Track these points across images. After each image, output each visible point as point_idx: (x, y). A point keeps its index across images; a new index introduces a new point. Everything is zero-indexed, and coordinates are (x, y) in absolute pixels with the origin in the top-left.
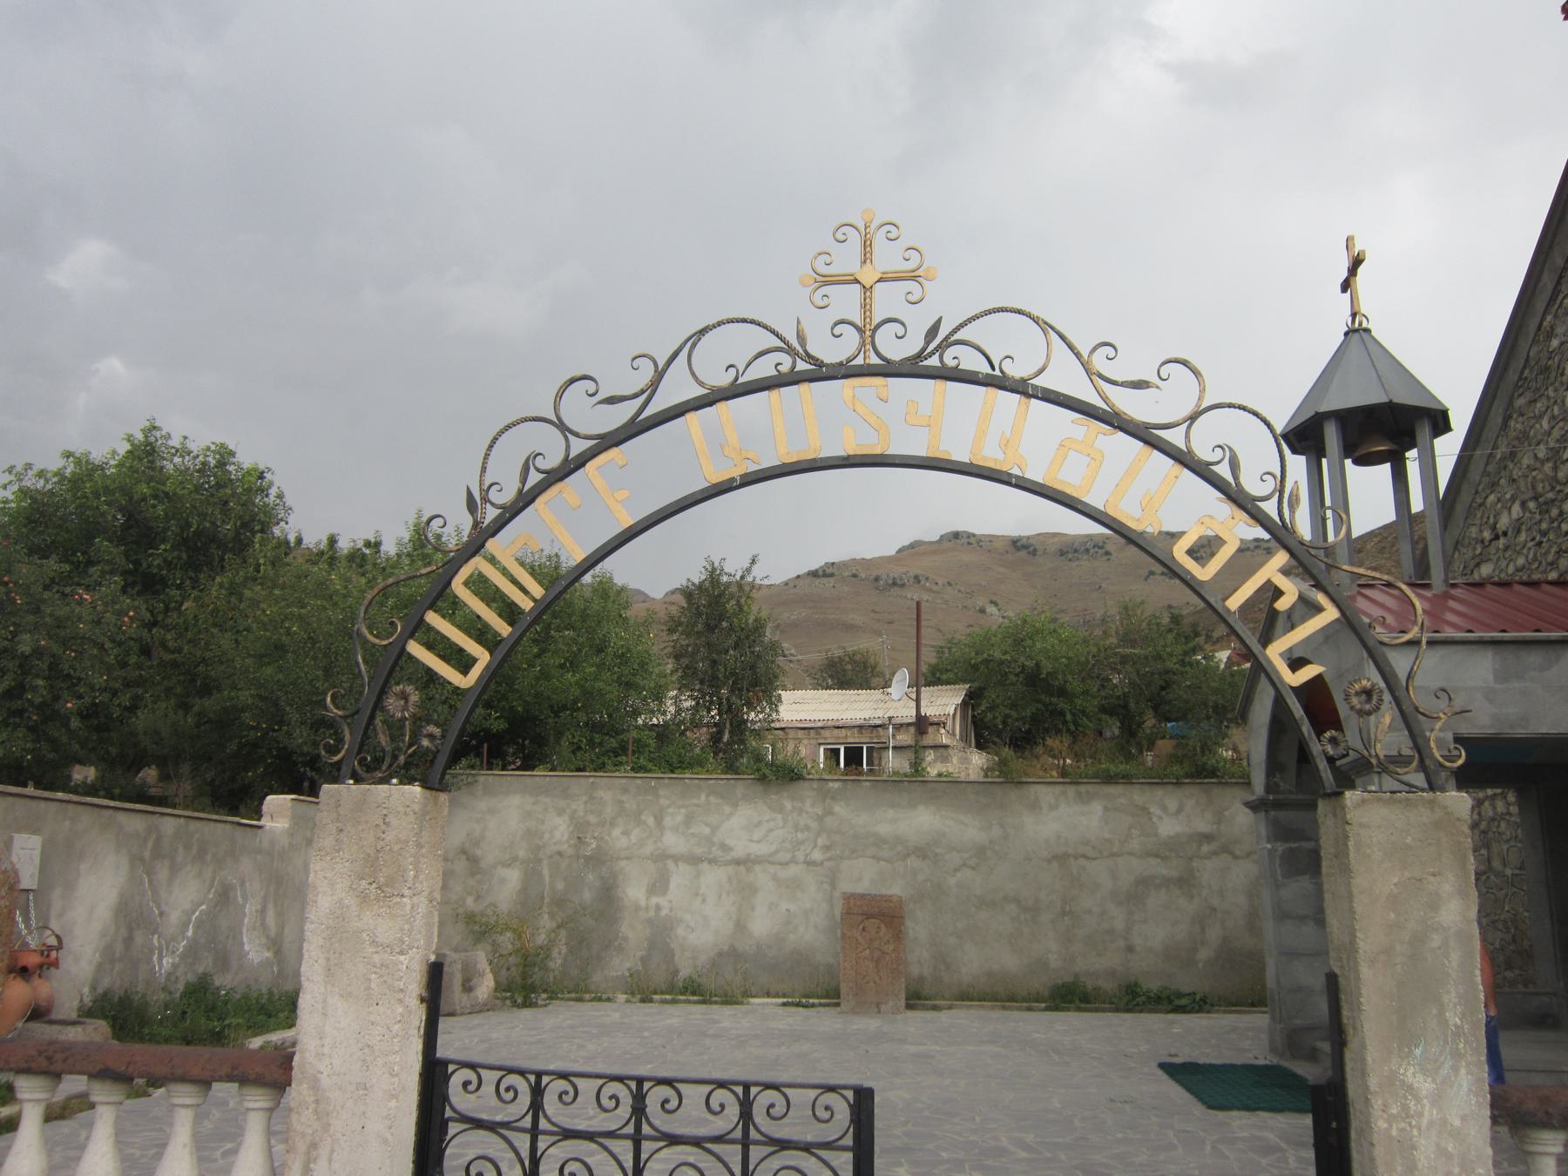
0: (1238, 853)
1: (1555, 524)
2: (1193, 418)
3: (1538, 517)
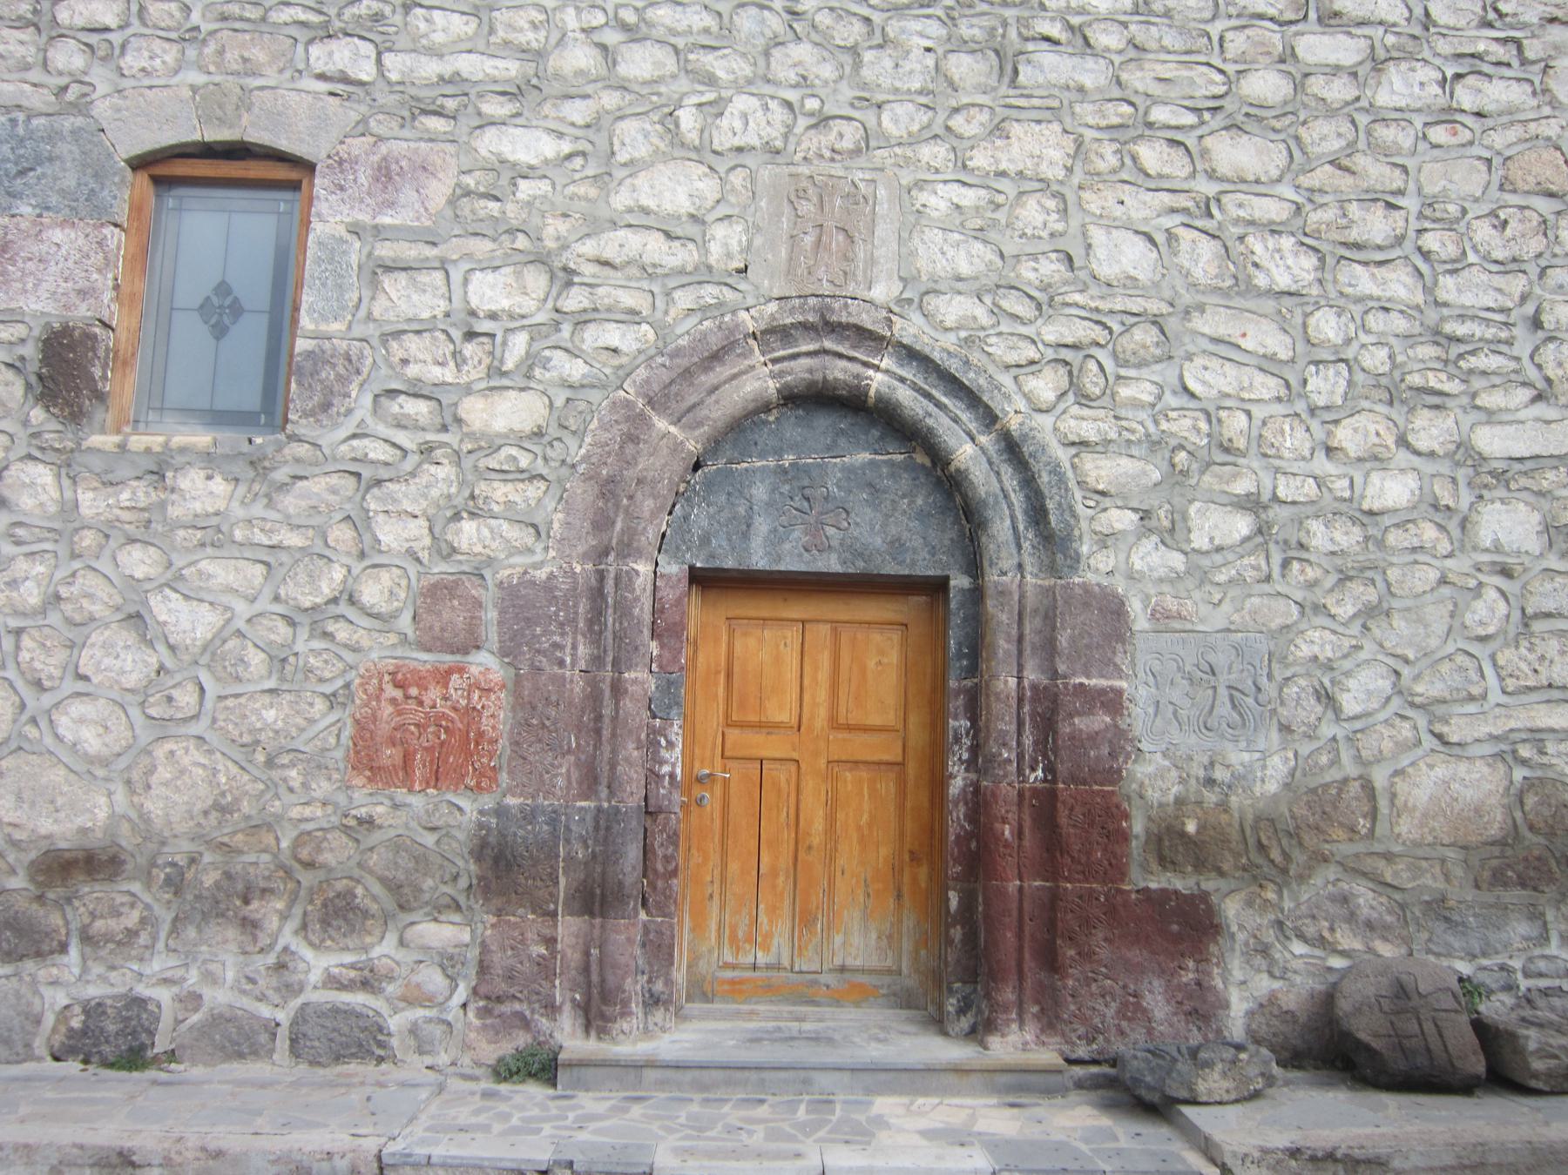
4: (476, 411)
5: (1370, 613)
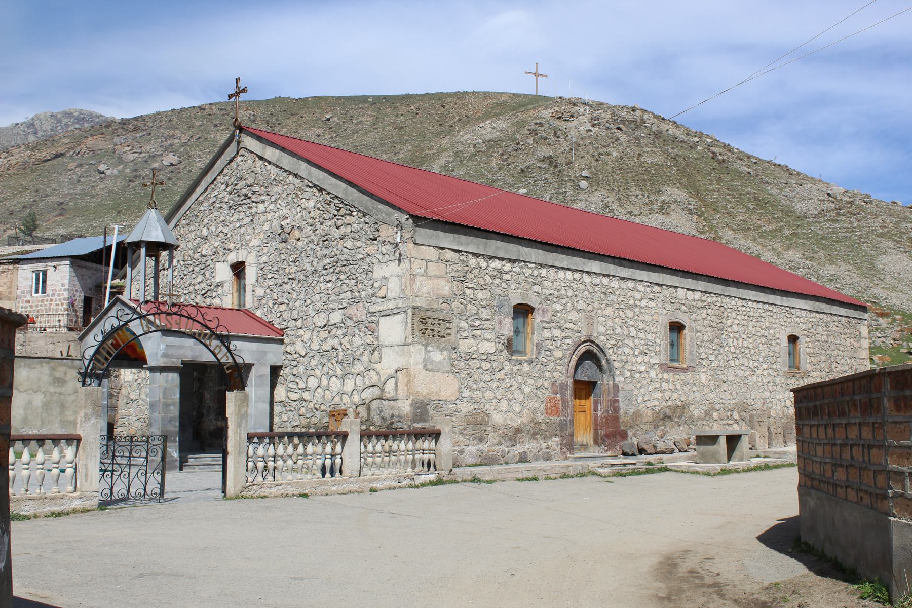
0: (21, 389)
1: (190, 273)
2: (217, 328)
3: (184, 268)
4: (555, 353)
5: (641, 387)
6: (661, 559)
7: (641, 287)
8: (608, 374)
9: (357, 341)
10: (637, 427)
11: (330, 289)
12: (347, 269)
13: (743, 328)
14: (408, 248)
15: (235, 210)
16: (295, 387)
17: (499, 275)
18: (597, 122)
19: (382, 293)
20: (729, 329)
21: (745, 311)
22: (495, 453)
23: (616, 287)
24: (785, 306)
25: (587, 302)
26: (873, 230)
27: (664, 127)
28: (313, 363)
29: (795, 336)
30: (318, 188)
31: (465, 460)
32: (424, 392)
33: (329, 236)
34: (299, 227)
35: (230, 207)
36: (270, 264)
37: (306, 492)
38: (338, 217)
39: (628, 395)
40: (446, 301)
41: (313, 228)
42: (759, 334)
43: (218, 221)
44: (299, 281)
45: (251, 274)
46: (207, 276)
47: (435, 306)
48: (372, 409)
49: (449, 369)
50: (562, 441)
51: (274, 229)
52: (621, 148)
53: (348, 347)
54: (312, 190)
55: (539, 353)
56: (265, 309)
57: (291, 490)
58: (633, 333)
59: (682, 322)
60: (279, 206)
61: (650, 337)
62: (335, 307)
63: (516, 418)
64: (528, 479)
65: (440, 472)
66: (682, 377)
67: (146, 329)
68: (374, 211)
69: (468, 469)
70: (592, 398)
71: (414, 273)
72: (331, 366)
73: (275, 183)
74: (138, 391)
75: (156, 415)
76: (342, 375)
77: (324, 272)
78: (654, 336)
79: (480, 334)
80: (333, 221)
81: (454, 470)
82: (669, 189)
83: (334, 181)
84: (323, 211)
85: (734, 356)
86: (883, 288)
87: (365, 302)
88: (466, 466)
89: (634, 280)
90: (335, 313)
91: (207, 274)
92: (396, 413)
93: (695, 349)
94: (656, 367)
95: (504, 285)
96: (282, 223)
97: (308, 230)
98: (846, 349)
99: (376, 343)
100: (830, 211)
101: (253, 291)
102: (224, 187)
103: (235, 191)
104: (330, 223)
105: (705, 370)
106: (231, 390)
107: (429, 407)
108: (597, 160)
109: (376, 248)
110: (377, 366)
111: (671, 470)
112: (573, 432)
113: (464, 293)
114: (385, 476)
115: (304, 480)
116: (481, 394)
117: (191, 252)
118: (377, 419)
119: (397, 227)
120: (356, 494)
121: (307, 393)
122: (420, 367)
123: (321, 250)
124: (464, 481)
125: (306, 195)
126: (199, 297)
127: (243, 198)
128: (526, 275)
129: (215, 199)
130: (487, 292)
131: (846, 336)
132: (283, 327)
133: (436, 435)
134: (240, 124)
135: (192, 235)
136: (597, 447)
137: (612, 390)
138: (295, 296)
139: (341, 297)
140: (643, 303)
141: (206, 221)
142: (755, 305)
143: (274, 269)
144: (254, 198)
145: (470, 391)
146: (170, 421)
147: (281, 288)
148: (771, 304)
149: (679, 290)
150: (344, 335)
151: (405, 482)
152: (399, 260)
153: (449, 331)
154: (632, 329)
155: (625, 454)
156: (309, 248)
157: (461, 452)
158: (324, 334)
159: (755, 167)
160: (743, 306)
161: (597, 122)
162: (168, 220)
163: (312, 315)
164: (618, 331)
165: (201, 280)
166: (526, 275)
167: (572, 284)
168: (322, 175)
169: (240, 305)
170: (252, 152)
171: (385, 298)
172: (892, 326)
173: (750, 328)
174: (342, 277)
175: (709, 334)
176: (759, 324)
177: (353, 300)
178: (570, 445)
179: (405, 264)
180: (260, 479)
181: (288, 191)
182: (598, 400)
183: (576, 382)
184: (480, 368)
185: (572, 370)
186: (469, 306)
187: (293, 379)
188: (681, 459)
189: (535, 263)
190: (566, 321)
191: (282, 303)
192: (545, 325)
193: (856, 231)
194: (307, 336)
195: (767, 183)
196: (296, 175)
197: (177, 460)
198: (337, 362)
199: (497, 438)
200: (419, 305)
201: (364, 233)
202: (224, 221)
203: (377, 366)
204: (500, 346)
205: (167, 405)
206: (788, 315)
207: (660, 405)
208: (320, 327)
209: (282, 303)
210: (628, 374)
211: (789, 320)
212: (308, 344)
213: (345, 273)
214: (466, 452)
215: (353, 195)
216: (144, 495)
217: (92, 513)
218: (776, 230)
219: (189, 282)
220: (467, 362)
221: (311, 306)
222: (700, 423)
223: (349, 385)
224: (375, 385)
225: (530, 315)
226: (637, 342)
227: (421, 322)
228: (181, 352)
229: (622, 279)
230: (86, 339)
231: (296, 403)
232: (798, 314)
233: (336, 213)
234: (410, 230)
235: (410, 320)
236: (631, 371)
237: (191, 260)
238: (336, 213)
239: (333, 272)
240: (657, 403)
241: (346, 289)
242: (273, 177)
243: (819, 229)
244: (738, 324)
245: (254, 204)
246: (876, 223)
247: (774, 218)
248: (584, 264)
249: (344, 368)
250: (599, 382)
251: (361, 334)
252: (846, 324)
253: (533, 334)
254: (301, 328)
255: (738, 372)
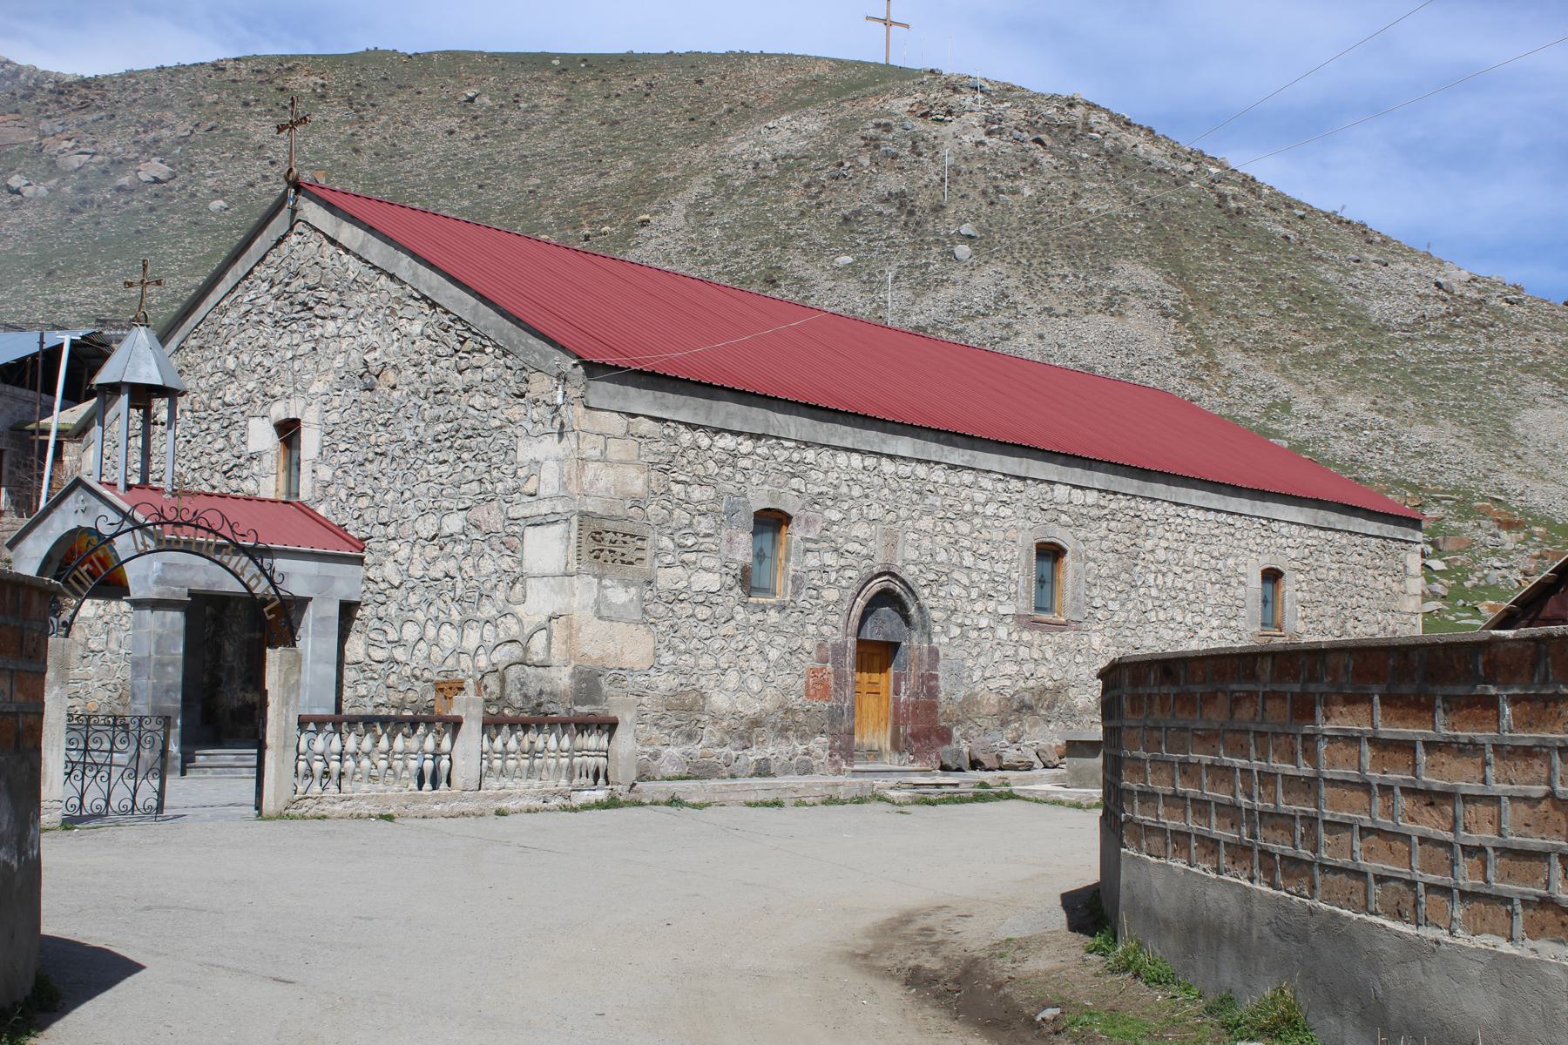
1: (203, 434)
3: (192, 425)
4: (825, 593)
5: (979, 654)
6: (897, 915)
7: (986, 482)
8: (919, 630)
9: (487, 565)
10: (969, 722)
11: (445, 475)
12: (473, 443)
13: (1175, 556)
14: (575, 415)
15: (285, 327)
16: (381, 638)
17: (730, 461)
18: (996, 126)
19: (530, 488)
20: (1148, 556)
21: (1181, 525)
22: (714, 759)
23: (941, 481)
24: (1259, 517)
25: (887, 507)
26: (1515, 358)
27: (1129, 139)
28: (413, 599)
29: (1277, 570)
30: (429, 302)
31: (662, 770)
32: (595, 654)
33: (445, 385)
34: (394, 367)
35: (276, 322)
36: (344, 426)
37: (391, 811)
38: (461, 354)
39: (955, 667)
40: (637, 503)
41: (418, 369)
42: (1206, 566)
43: (255, 344)
44: (393, 459)
45: (310, 441)
46: (234, 440)
47: (619, 512)
48: (508, 681)
49: (640, 618)
50: (832, 742)
51: (353, 366)
52: (1040, 180)
53: (472, 574)
54: (418, 304)
55: (796, 593)
56: (334, 504)
57: (366, 808)
58: (968, 560)
59: (1060, 542)
60: (361, 328)
61: (999, 568)
62: (451, 506)
63: (752, 701)
64: (766, 804)
65: (615, 787)
66: (1057, 639)
67: (141, 547)
68: (522, 347)
69: (666, 783)
70: (891, 671)
71: (584, 456)
72: (442, 606)
73: (355, 287)
74: (104, 637)
75: (143, 681)
76: (461, 621)
77: (435, 445)
78: (1006, 566)
79: (693, 559)
80: (453, 360)
81: (639, 785)
82: (1127, 265)
83: (455, 291)
84: (436, 341)
85: (1157, 603)
86: (1520, 472)
87: (502, 501)
88: (664, 779)
89: (973, 469)
90: (452, 516)
91: (233, 438)
92: (547, 688)
93: (1082, 590)
94: (1009, 620)
95: (739, 477)
96: (365, 357)
97: (410, 372)
98: (1377, 595)
99: (518, 570)
100: (1437, 319)
101: (314, 471)
102: (266, 285)
103: (286, 295)
104: (447, 364)
105: (1101, 626)
106: (274, 646)
107: (602, 679)
108: (992, 203)
109: (523, 411)
110: (519, 609)
111: (1018, 797)
112: (853, 729)
113: (669, 489)
114: (520, 791)
115: (389, 793)
116: (693, 660)
117: (205, 397)
118: (515, 696)
119: (558, 377)
120: (473, 818)
121: (401, 649)
122: (590, 613)
123: (431, 408)
124: (655, 803)
125: (407, 312)
126: (217, 476)
127: (299, 308)
128: (779, 460)
129: (250, 307)
130: (709, 489)
131: (1376, 573)
132: (363, 535)
133: (610, 726)
134: (297, 178)
135: (208, 367)
136: (897, 756)
137: (925, 658)
138: (384, 484)
139: (462, 491)
140: (990, 510)
141: (233, 344)
142: (1201, 515)
143: (351, 435)
144: (318, 310)
145: (674, 654)
146: (167, 691)
147: (362, 468)
148: (1233, 513)
149: (1057, 487)
150: (466, 555)
151: (555, 802)
152: (561, 434)
153: (640, 554)
154: (967, 554)
155: (945, 768)
156: (411, 404)
157: (655, 756)
158: (432, 551)
159: (1301, 225)
160: (1178, 516)
161: (996, 126)
162: (163, 339)
163: (413, 517)
164: (942, 556)
165: (221, 447)
166: (780, 460)
167: (860, 477)
168: (436, 279)
169: (289, 494)
170: (317, 230)
171: (535, 495)
172: (1524, 547)
173: (1190, 554)
174: (465, 456)
175: (1111, 565)
176: (1206, 549)
177: (481, 497)
178: (845, 749)
179: (570, 441)
180: (316, 788)
181: (378, 303)
182: (901, 675)
183: (861, 643)
184: (693, 616)
185: (855, 622)
186: (677, 512)
187: (378, 624)
188: (1041, 780)
189: (796, 441)
190: (846, 539)
191: (363, 495)
192: (809, 545)
193: (1483, 360)
194: (404, 552)
195: (1320, 258)
196: (392, 277)
197: (176, 758)
198: (453, 600)
199: (718, 735)
200: (591, 509)
201: (503, 383)
202: (264, 346)
203: (519, 609)
204: (729, 581)
205: (162, 665)
206: (1264, 533)
207: (1014, 685)
208: (426, 539)
209: (363, 495)
210: (956, 631)
211: (1266, 542)
212: (405, 567)
213: (470, 449)
214: (663, 756)
215: (488, 319)
216: (133, 809)
217: (52, 833)
218: (1327, 353)
219: (200, 449)
220: (670, 606)
221: (411, 502)
222: (1087, 718)
223: (472, 639)
224: (515, 641)
225: (784, 527)
226: (975, 576)
227: (594, 538)
228: (188, 575)
229: (953, 467)
230: (19, 546)
231: (382, 666)
232: (1285, 531)
233: (458, 346)
234: (578, 385)
235: (574, 535)
236: (961, 626)
237: (206, 410)
238: (458, 346)
239: (451, 447)
240: (1008, 683)
241: (472, 477)
242: (352, 276)
243: (1412, 353)
244: (1166, 549)
245: (319, 320)
246: (1523, 345)
247: (1325, 329)
248: (884, 442)
249: (464, 609)
250: (904, 644)
251: (493, 553)
252: (1378, 550)
253: (787, 560)
254: (394, 539)
255: (1163, 632)
